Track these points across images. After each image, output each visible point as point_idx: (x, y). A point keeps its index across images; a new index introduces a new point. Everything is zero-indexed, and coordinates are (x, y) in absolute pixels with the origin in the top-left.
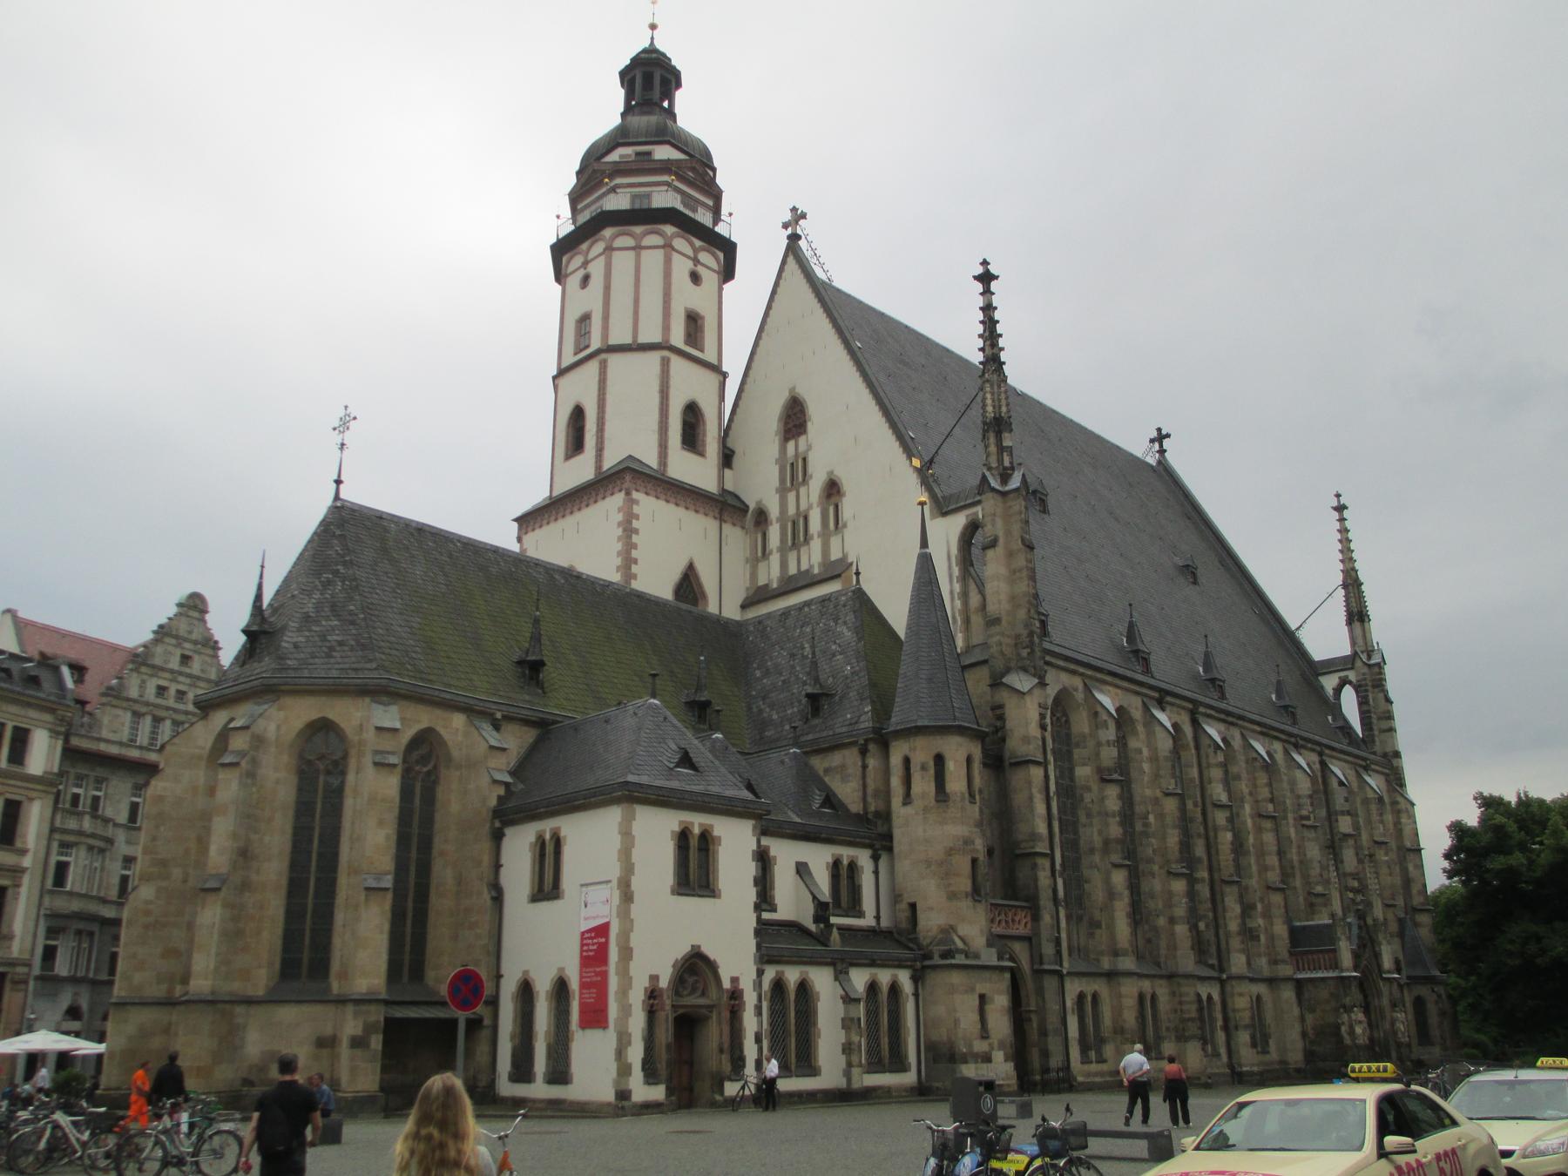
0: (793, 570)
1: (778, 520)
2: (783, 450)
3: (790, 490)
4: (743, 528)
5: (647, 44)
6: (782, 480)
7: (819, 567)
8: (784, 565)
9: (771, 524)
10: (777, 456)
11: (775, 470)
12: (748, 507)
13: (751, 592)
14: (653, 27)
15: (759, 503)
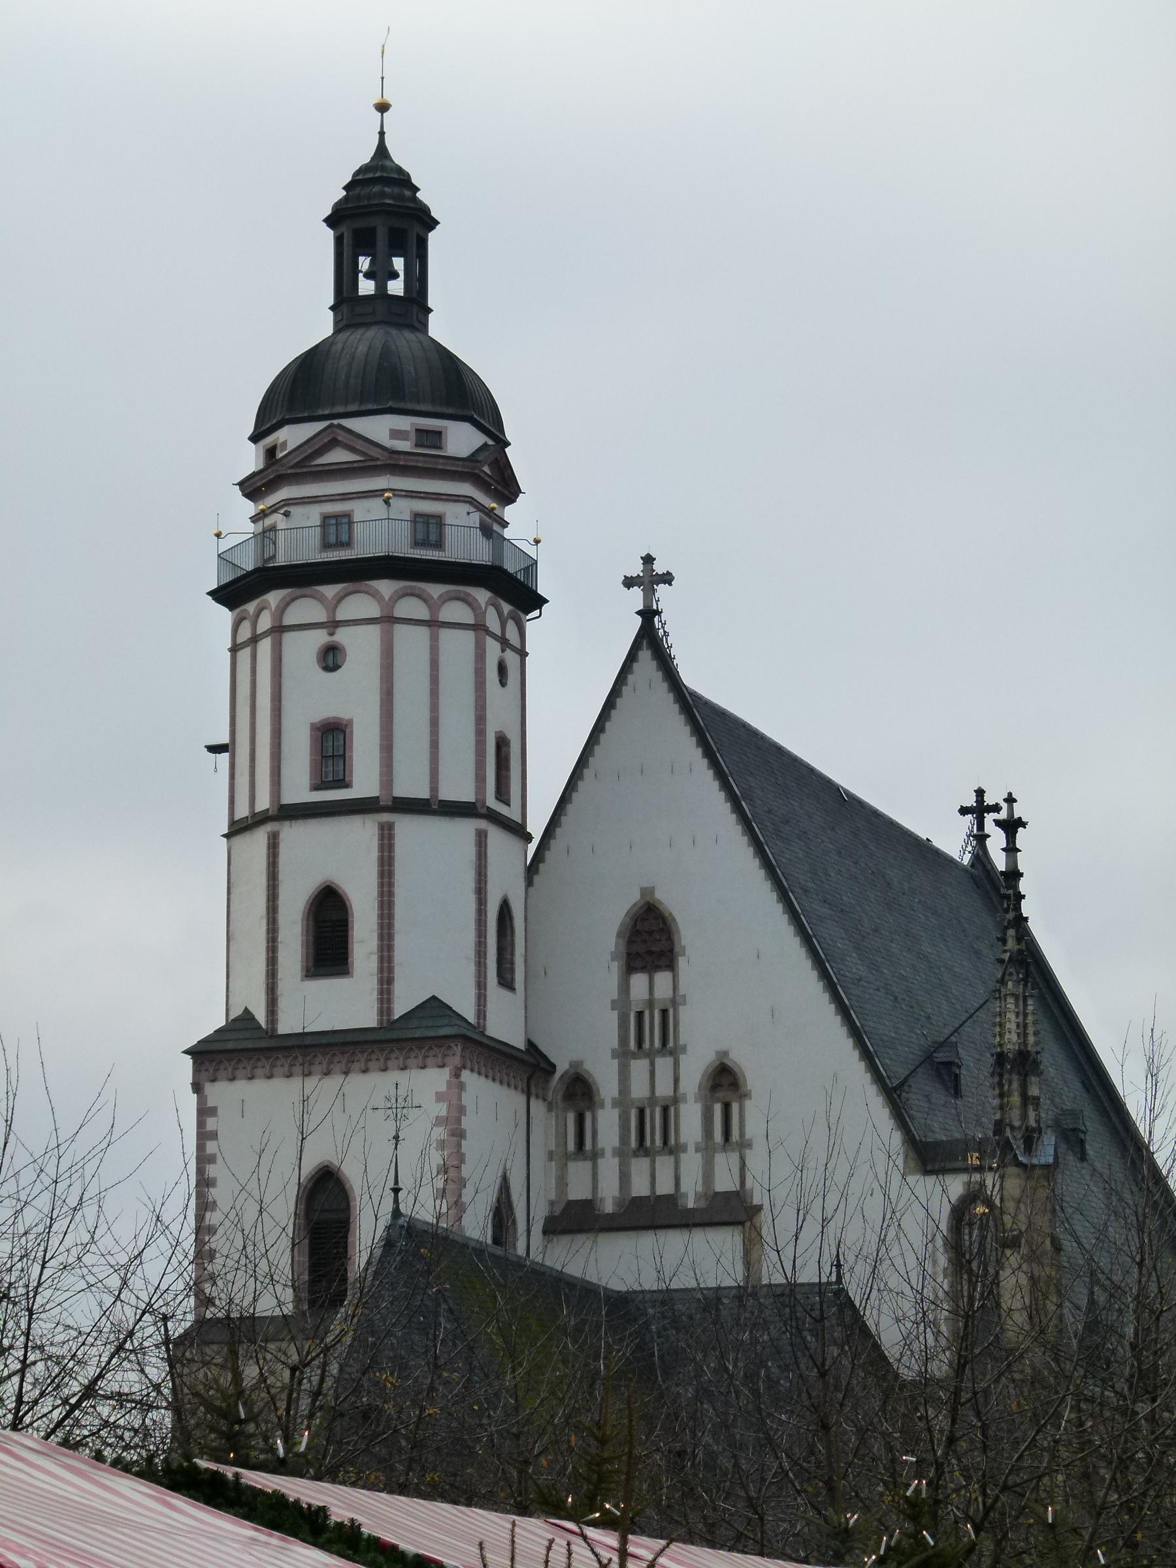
0: (640, 1188)
1: (616, 1103)
2: (625, 988)
3: (634, 1056)
4: (545, 1100)
5: (365, 155)
6: (623, 1040)
7: (698, 1197)
8: (625, 1178)
9: (602, 1106)
10: (615, 996)
11: (612, 1019)
12: (553, 1066)
13: (558, 1210)
14: (383, 108)
15: (575, 1065)
